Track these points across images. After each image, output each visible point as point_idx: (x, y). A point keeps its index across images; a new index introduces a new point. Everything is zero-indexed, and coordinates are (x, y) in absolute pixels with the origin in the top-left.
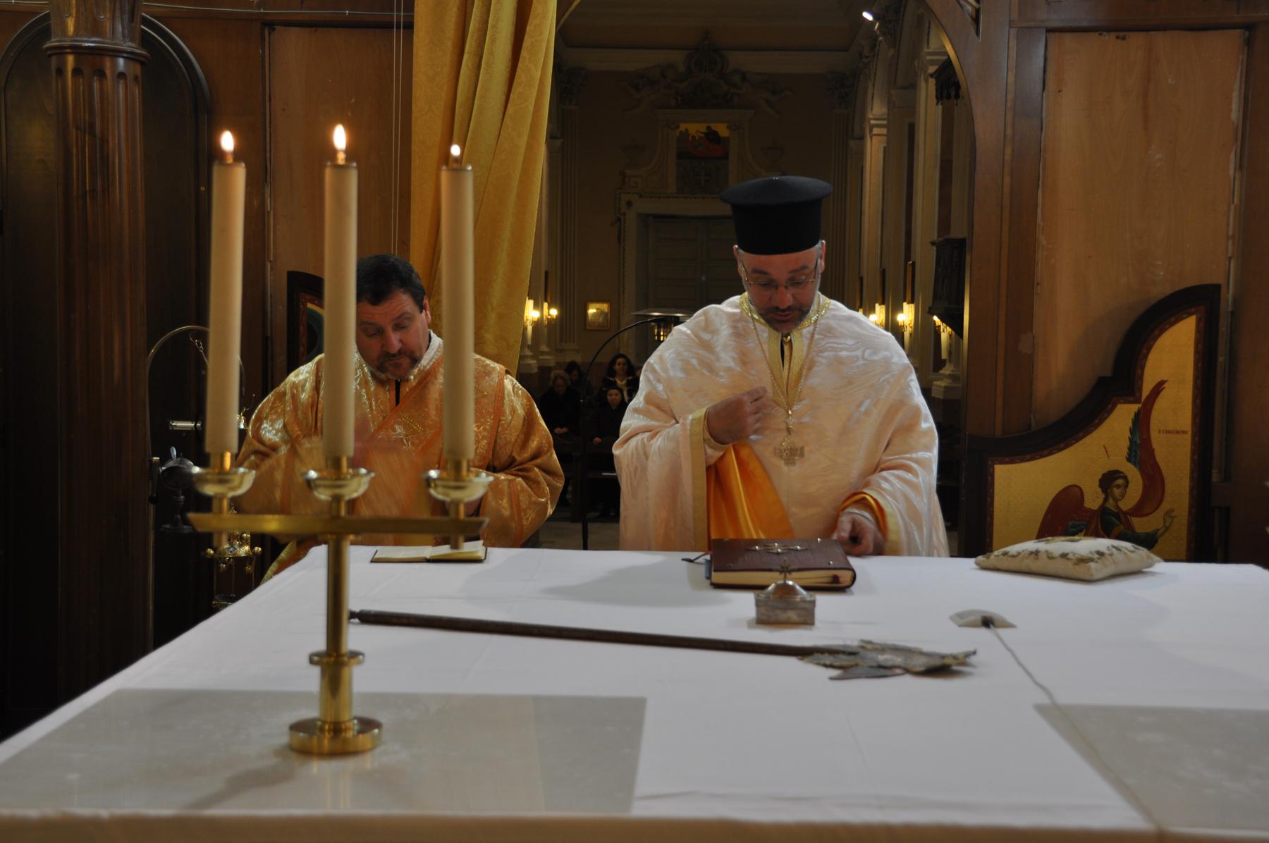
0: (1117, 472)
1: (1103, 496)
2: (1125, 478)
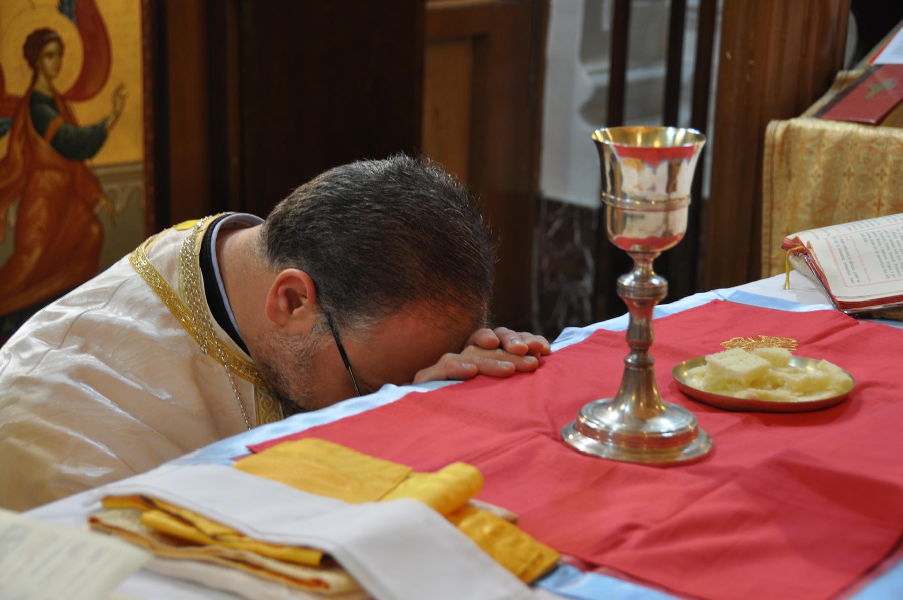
1: (28, 73)
2: (58, 40)
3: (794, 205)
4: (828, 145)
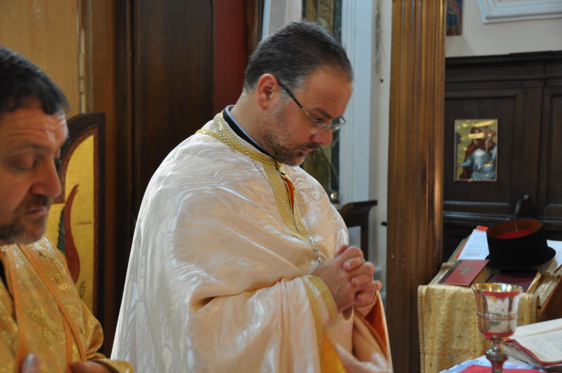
3: (434, 325)
4: (448, 296)
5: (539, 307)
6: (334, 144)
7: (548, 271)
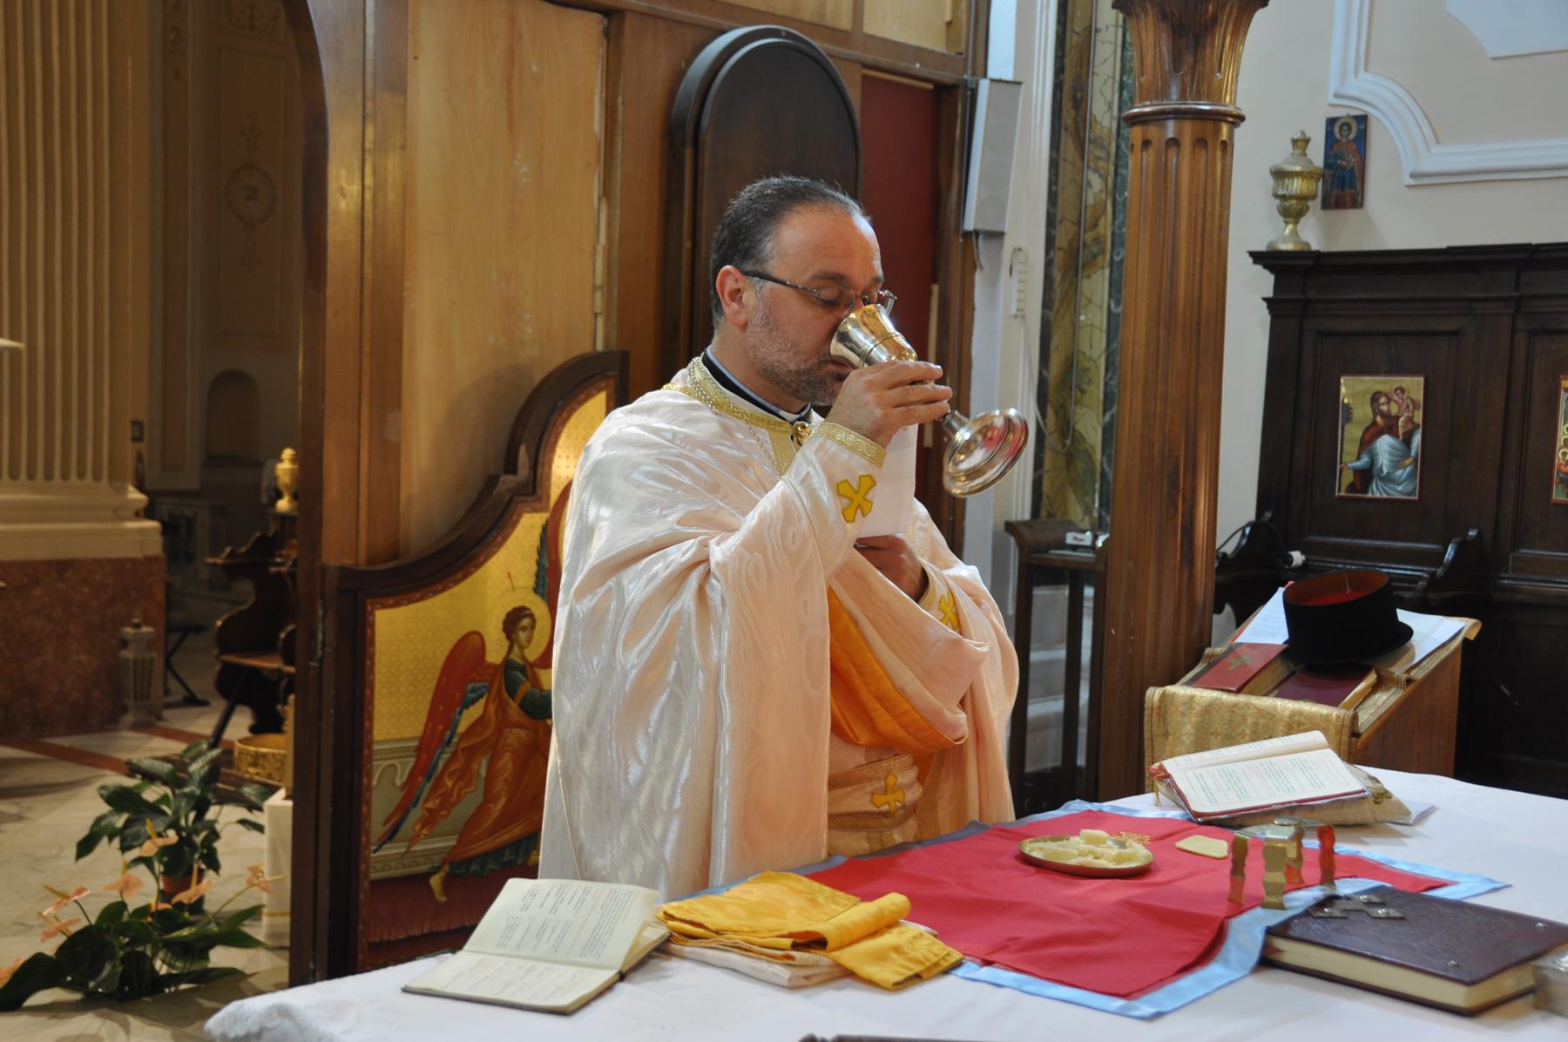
0: (522, 609)
1: (506, 644)
2: (532, 616)
5: (1355, 734)
6: (1107, 418)
7: (1393, 669)
